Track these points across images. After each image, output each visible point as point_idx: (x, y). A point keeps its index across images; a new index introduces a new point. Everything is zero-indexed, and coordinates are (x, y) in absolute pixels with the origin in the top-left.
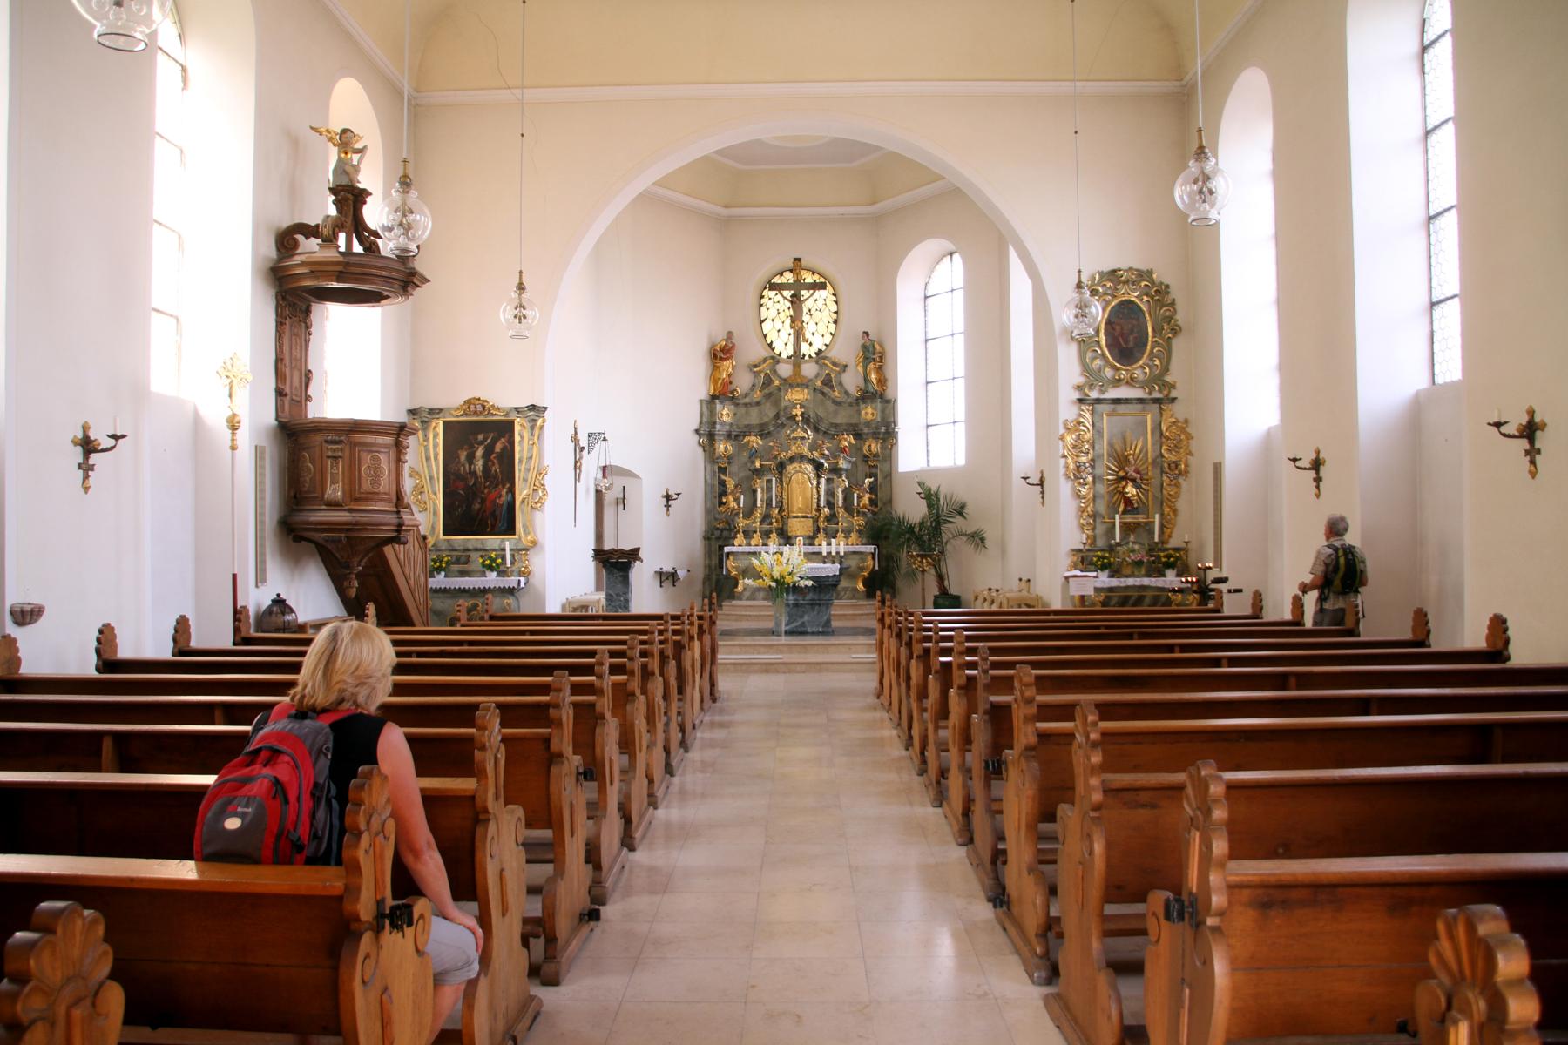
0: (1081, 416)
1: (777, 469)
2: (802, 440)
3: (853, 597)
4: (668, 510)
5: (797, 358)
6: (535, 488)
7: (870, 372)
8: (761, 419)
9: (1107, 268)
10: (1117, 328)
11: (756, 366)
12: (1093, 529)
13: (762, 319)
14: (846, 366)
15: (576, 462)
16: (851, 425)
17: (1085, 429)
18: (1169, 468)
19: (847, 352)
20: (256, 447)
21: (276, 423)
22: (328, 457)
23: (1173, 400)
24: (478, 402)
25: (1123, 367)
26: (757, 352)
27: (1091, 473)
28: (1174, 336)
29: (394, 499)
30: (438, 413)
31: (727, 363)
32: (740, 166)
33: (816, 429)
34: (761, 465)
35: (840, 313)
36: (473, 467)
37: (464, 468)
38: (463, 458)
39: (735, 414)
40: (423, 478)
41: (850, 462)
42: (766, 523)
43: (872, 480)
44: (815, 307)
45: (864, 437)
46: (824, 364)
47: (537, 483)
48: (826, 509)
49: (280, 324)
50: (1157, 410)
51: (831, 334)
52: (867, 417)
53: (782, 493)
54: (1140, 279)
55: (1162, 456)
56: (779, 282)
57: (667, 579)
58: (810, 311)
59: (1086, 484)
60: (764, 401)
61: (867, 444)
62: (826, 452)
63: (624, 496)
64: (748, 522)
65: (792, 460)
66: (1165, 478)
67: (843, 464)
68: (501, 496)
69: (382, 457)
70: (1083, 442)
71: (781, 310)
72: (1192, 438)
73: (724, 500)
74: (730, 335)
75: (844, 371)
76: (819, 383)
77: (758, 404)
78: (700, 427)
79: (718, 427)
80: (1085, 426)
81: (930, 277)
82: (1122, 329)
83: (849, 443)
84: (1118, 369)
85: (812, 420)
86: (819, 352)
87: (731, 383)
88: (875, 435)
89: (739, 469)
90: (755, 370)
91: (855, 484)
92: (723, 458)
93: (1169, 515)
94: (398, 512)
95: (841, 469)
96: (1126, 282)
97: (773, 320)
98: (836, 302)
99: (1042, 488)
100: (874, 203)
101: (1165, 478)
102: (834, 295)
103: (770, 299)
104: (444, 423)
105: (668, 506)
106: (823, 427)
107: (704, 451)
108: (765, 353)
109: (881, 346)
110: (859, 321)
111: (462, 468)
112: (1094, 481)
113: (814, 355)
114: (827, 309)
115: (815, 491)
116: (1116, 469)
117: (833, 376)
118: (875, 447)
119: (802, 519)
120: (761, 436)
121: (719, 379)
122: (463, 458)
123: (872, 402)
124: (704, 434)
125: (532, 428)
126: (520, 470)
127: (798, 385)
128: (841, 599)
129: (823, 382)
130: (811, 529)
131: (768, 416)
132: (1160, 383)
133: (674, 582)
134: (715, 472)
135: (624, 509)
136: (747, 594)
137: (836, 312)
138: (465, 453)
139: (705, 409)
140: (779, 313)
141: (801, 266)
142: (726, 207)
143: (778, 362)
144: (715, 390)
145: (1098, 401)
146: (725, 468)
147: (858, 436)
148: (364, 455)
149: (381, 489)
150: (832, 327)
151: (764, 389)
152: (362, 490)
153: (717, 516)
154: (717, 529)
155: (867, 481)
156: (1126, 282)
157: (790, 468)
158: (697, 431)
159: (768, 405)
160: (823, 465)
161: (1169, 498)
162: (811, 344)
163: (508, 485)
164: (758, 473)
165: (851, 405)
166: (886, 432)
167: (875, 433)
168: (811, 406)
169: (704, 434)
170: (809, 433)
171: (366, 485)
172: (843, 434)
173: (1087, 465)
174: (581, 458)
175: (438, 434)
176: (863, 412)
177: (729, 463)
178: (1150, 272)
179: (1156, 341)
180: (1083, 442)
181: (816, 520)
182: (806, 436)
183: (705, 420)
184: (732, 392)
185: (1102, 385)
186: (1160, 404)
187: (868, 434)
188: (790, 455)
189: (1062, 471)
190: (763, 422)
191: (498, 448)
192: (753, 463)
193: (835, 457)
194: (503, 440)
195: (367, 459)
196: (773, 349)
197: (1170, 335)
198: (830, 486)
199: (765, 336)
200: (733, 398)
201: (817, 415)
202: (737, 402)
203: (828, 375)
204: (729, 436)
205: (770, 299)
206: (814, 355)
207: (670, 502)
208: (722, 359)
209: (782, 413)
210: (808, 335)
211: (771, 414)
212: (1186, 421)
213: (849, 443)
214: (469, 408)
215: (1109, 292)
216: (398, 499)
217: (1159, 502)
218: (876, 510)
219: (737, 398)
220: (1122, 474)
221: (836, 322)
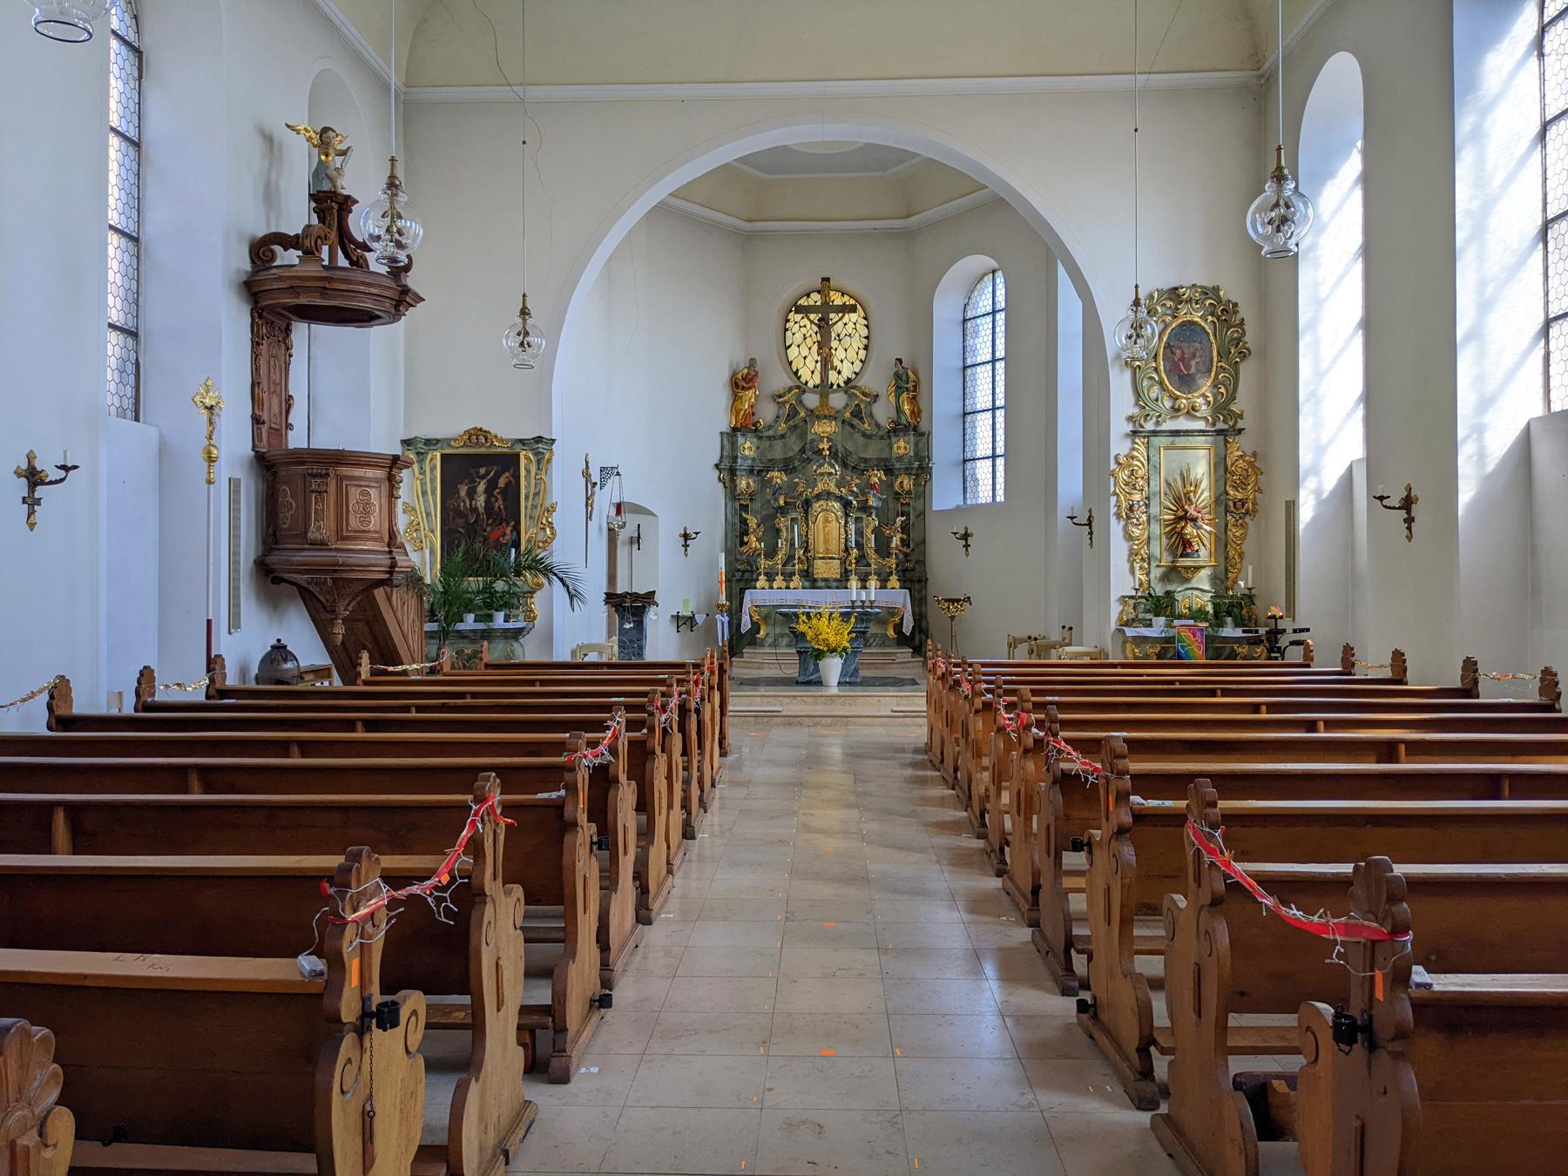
0: (1137, 450)
1: (803, 507)
2: (828, 476)
3: (883, 645)
4: (686, 550)
5: (824, 388)
6: (542, 526)
7: (903, 402)
8: (786, 453)
9: (1166, 286)
10: (1178, 352)
11: (780, 396)
12: (1148, 574)
13: (787, 345)
14: (877, 396)
15: (588, 499)
16: (882, 459)
17: (1140, 465)
18: (1235, 507)
19: (878, 381)
20: (230, 479)
21: (253, 453)
22: (313, 491)
23: (1240, 431)
24: (480, 433)
25: (1185, 396)
26: (777, 380)
27: (1146, 513)
28: (1242, 360)
29: (386, 539)
30: (436, 443)
31: (751, 392)
32: (769, 177)
33: (844, 465)
35: (872, 338)
36: (474, 502)
37: (465, 504)
38: (463, 493)
40: (419, 515)
42: (791, 564)
44: (845, 332)
45: (897, 473)
47: (544, 521)
48: (855, 550)
49: (256, 344)
50: (1223, 442)
51: (861, 361)
53: (807, 532)
54: (1203, 297)
55: (1227, 494)
56: (806, 304)
57: (685, 624)
58: (838, 336)
59: (1139, 525)
60: (789, 433)
61: (899, 480)
62: (855, 489)
63: (639, 534)
64: (771, 563)
65: (818, 497)
66: (1229, 518)
67: (872, 502)
68: (505, 535)
69: (373, 492)
70: (1136, 478)
71: (808, 335)
72: (1262, 473)
73: (746, 540)
74: (752, 363)
75: (875, 401)
77: (782, 436)
78: (721, 461)
79: (739, 461)
80: (1139, 461)
81: (970, 298)
82: (1183, 353)
83: (880, 479)
84: (1176, 398)
85: (840, 455)
86: (848, 381)
87: (753, 414)
88: (908, 471)
90: (780, 400)
91: (885, 521)
93: (1234, 558)
94: (391, 552)
95: (871, 507)
96: (1189, 301)
97: (799, 346)
98: (867, 326)
99: (1090, 528)
100: (908, 216)
101: (1229, 518)
102: (865, 318)
104: (442, 455)
105: (686, 546)
106: (852, 461)
107: (725, 487)
108: (789, 382)
110: (892, 347)
111: (462, 504)
112: (1149, 521)
113: (842, 384)
114: (857, 334)
115: (842, 530)
116: (1175, 508)
118: (907, 483)
120: (785, 471)
121: (741, 410)
122: (463, 493)
123: (905, 435)
124: (725, 469)
125: (539, 462)
126: (526, 508)
127: (825, 417)
128: (870, 646)
130: (839, 570)
131: (793, 449)
132: (1225, 412)
133: (692, 627)
135: (639, 549)
136: (770, 640)
137: (867, 338)
138: (466, 488)
139: (726, 442)
140: (805, 339)
141: (829, 287)
142: (749, 221)
143: (804, 392)
145: (1155, 433)
146: (747, 506)
147: (889, 471)
148: (352, 490)
149: (371, 527)
150: (862, 353)
152: (350, 529)
153: (738, 557)
154: (739, 570)
155: (900, 519)
156: (1189, 301)
157: (816, 506)
158: (717, 466)
159: (793, 437)
161: (1234, 540)
162: (839, 373)
163: (513, 523)
164: (783, 511)
165: (882, 438)
166: (921, 468)
167: (907, 469)
168: (839, 439)
170: (837, 468)
171: (354, 523)
172: (873, 470)
173: (1141, 503)
174: (593, 494)
175: (436, 466)
177: (751, 500)
178: (1216, 290)
179: (1221, 367)
180: (1136, 478)
181: (843, 562)
182: (834, 472)
184: (754, 425)
185: (1160, 416)
186: (1225, 436)
187: (900, 469)
188: (816, 492)
189: (1113, 510)
191: (502, 482)
192: (777, 500)
193: (864, 494)
194: (507, 474)
195: (355, 494)
196: (799, 378)
197: (1238, 360)
199: (790, 363)
200: (756, 430)
201: (846, 449)
202: (761, 435)
203: (858, 405)
204: (751, 471)
205: (796, 323)
206: (842, 384)
207: (689, 542)
208: (743, 388)
209: (808, 446)
210: (836, 363)
211: (797, 449)
212: (1255, 455)
214: (469, 439)
215: (1169, 312)
216: (390, 538)
217: (1223, 545)
218: (908, 551)
220: (1181, 513)
221: (866, 348)
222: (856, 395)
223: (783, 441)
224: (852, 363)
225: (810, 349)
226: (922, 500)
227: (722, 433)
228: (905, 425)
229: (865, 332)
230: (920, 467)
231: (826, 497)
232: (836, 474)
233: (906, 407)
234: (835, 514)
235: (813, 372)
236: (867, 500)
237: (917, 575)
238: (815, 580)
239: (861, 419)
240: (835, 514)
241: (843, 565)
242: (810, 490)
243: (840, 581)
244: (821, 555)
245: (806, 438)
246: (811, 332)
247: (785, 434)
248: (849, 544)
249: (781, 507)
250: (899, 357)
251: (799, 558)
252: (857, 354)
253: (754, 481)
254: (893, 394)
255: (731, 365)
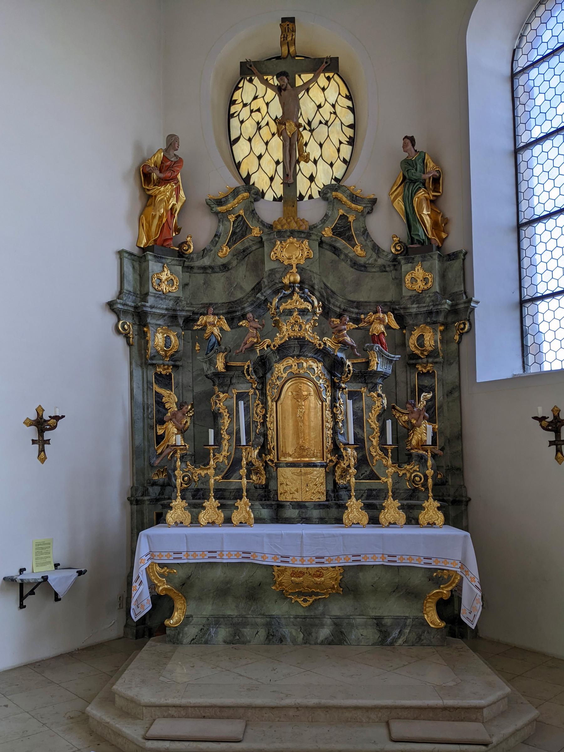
4: (42, 450)
8: (231, 294)
13: (233, 138)
14: (374, 202)
34: (227, 367)
35: (360, 128)
39: (185, 286)
41: (391, 361)
43: (429, 396)
44: (318, 118)
46: (336, 198)
51: (344, 161)
52: (416, 287)
53: (265, 417)
58: (309, 123)
60: (235, 263)
61: (416, 334)
62: (348, 339)
71: (263, 123)
75: (372, 210)
76: (327, 232)
77: (225, 267)
79: (151, 300)
83: (388, 327)
87: (178, 230)
89: (194, 379)
90: (219, 209)
92: (162, 358)
95: (376, 374)
97: (250, 140)
98: (352, 109)
102: (349, 97)
103: (245, 105)
106: (338, 304)
107: (129, 344)
108: (236, 183)
109: (436, 162)
114: (337, 122)
115: (328, 414)
117: (351, 219)
119: (304, 470)
121: (154, 217)
124: (125, 312)
127: (292, 233)
129: (335, 230)
130: (323, 488)
131: (241, 288)
134: (149, 383)
136: (192, 631)
137: (352, 126)
140: (259, 128)
144: (148, 240)
150: (346, 151)
151: (235, 243)
160: (342, 363)
162: (312, 179)
165: (383, 269)
167: (430, 313)
168: (316, 269)
169: (125, 312)
170: (316, 303)
172: (376, 312)
176: (408, 277)
182: (310, 308)
183: (128, 287)
184: (180, 246)
187: (416, 314)
190: (232, 299)
192: (212, 362)
198: (357, 405)
199: (238, 166)
203: (343, 217)
205: (245, 105)
206: (316, 195)
207: (47, 435)
211: (248, 286)
213: (388, 327)
219: (190, 258)
221: (351, 141)
222: (340, 201)
223: (227, 274)
224: (331, 165)
225: (267, 143)
226: (455, 366)
227: (121, 253)
228: (422, 243)
229: (348, 118)
230: (454, 311)
231: (297, 352)
232: (315, 313)
233: (425, 212)
234: (315, 384)
235: (272, 179)
236: (368, 363)
237: (452, 491)
238: (280, 506)
239: (350, 239)
240: (315, 384)
241: (330, 477)
242: (268, 341)
243: (328, 507)
244: (290, 459)
245: (263, 269)
246: (267, 118)
247: (229, 263)
248: (341, 438)
249: (218, 374)
250: (410, 135)
251: (250, 464)
252: (338, 150)
253: (179, 336)
254: (400, 198)
255: (138, 147)
